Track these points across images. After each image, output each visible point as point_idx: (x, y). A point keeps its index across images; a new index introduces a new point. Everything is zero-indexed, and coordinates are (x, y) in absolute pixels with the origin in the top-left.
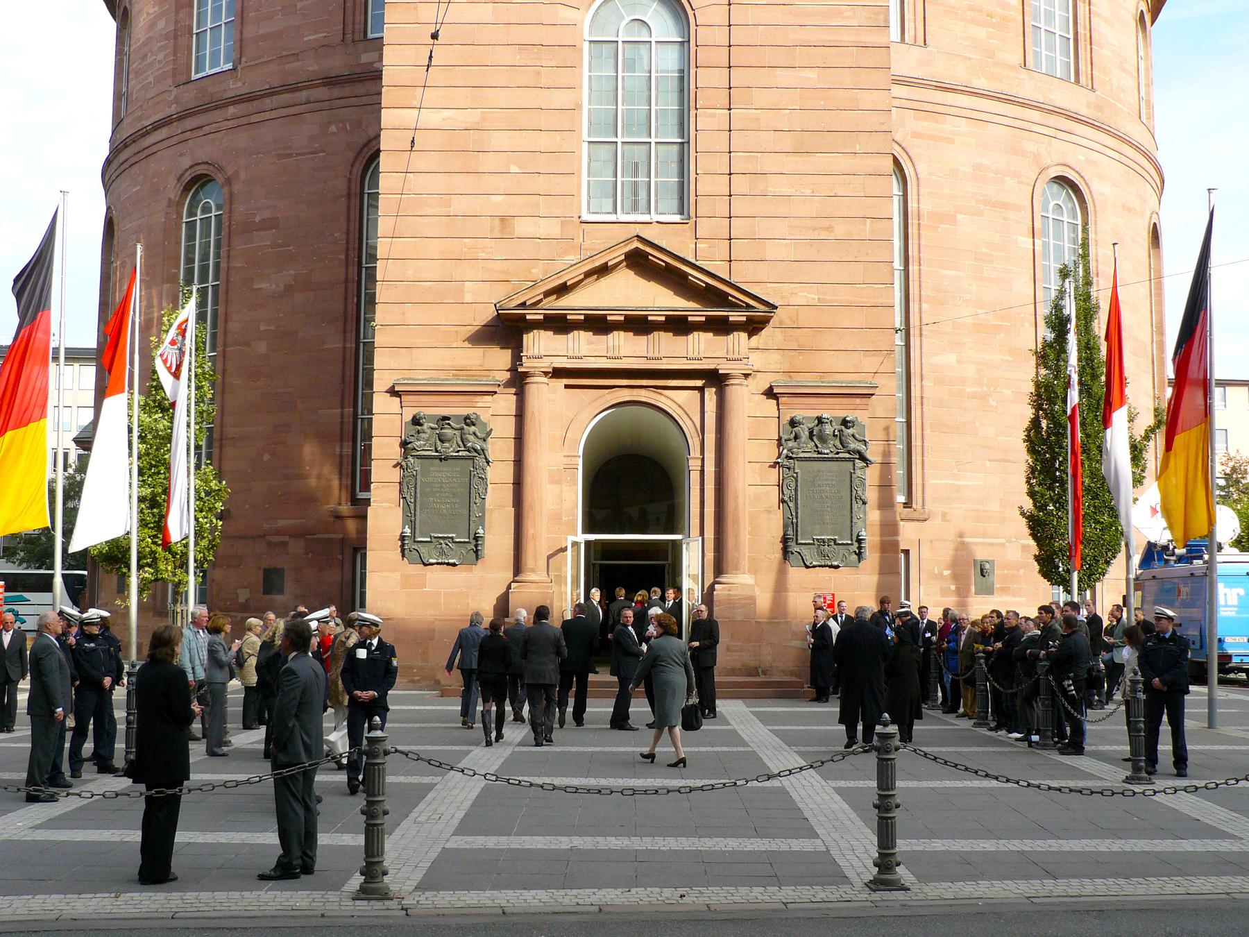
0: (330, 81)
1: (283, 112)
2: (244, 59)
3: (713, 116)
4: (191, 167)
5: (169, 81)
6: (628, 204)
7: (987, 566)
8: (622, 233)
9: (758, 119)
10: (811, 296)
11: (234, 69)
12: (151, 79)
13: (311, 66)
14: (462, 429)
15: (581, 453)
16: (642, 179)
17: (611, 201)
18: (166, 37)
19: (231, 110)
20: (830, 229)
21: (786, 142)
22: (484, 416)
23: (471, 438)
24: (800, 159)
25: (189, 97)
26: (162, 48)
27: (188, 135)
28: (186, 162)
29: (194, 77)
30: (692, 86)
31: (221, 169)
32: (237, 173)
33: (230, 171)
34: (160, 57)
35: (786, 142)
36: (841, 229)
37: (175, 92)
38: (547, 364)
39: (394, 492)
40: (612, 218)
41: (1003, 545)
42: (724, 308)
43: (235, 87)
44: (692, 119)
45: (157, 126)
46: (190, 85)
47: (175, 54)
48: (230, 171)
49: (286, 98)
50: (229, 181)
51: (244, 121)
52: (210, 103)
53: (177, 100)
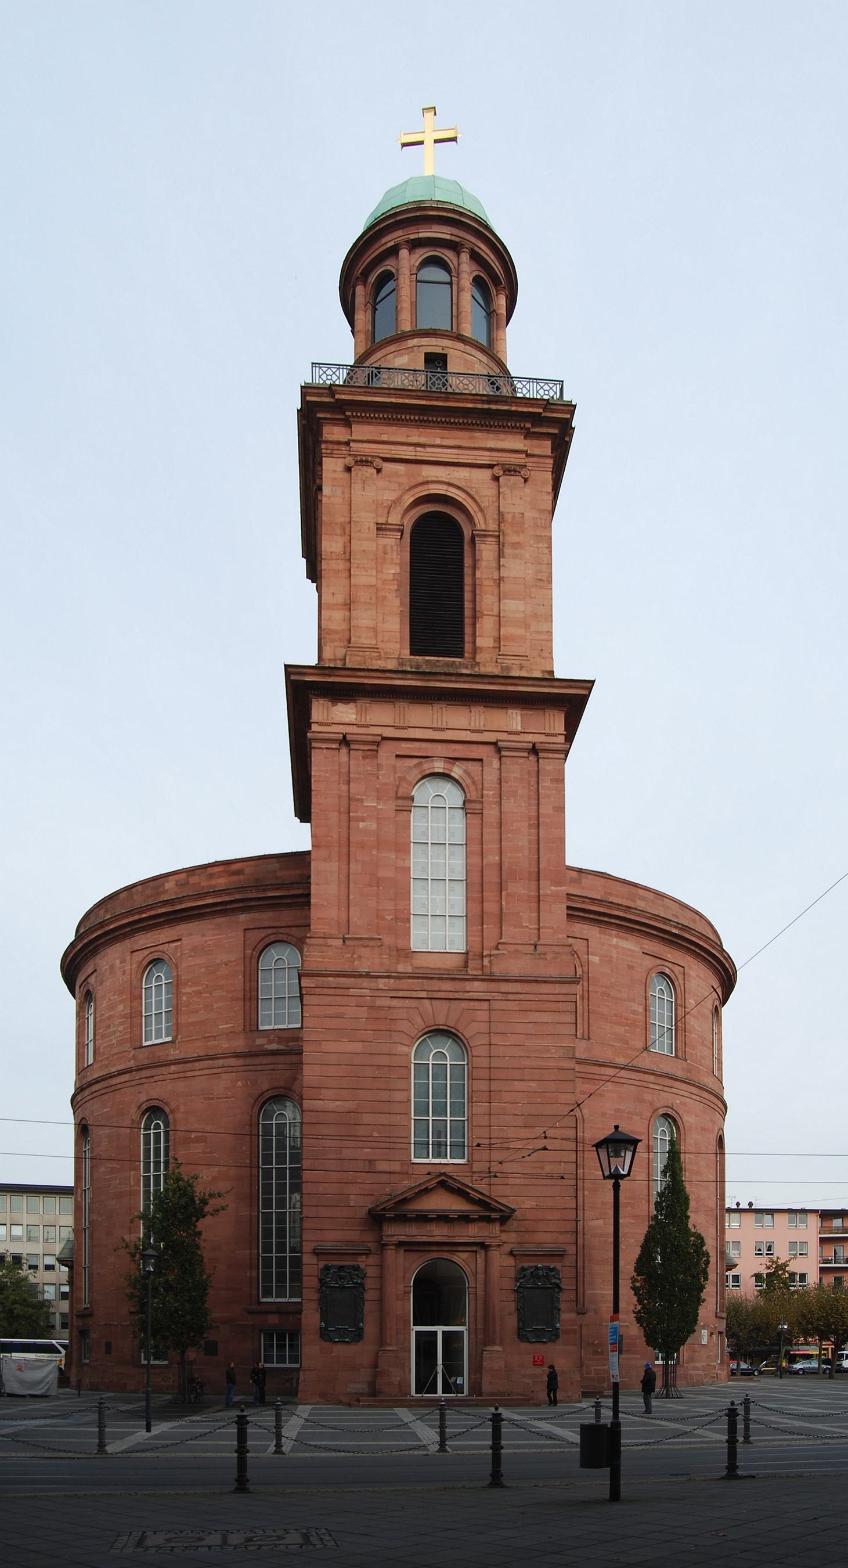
6: (435, 1153)
11: (172, 1042)
12: (114, 1041)
13: (225, 1045)
18: (125, 1016)
25: (143, 1057)
26: (121, 1024)
27: (144, 1081)
28: (143, 1098)
29: (145, 1044)
32: (178, 1107)
33: (173, 1105)
34: (121, 1028)
37: (133, 1052)
43: (174, 1053)
46: (143, 1050)
47: (131, 1027)
48: (173, 1105)
51: (181, 1075)
52: (156, 1063)
53: (134, 1058)
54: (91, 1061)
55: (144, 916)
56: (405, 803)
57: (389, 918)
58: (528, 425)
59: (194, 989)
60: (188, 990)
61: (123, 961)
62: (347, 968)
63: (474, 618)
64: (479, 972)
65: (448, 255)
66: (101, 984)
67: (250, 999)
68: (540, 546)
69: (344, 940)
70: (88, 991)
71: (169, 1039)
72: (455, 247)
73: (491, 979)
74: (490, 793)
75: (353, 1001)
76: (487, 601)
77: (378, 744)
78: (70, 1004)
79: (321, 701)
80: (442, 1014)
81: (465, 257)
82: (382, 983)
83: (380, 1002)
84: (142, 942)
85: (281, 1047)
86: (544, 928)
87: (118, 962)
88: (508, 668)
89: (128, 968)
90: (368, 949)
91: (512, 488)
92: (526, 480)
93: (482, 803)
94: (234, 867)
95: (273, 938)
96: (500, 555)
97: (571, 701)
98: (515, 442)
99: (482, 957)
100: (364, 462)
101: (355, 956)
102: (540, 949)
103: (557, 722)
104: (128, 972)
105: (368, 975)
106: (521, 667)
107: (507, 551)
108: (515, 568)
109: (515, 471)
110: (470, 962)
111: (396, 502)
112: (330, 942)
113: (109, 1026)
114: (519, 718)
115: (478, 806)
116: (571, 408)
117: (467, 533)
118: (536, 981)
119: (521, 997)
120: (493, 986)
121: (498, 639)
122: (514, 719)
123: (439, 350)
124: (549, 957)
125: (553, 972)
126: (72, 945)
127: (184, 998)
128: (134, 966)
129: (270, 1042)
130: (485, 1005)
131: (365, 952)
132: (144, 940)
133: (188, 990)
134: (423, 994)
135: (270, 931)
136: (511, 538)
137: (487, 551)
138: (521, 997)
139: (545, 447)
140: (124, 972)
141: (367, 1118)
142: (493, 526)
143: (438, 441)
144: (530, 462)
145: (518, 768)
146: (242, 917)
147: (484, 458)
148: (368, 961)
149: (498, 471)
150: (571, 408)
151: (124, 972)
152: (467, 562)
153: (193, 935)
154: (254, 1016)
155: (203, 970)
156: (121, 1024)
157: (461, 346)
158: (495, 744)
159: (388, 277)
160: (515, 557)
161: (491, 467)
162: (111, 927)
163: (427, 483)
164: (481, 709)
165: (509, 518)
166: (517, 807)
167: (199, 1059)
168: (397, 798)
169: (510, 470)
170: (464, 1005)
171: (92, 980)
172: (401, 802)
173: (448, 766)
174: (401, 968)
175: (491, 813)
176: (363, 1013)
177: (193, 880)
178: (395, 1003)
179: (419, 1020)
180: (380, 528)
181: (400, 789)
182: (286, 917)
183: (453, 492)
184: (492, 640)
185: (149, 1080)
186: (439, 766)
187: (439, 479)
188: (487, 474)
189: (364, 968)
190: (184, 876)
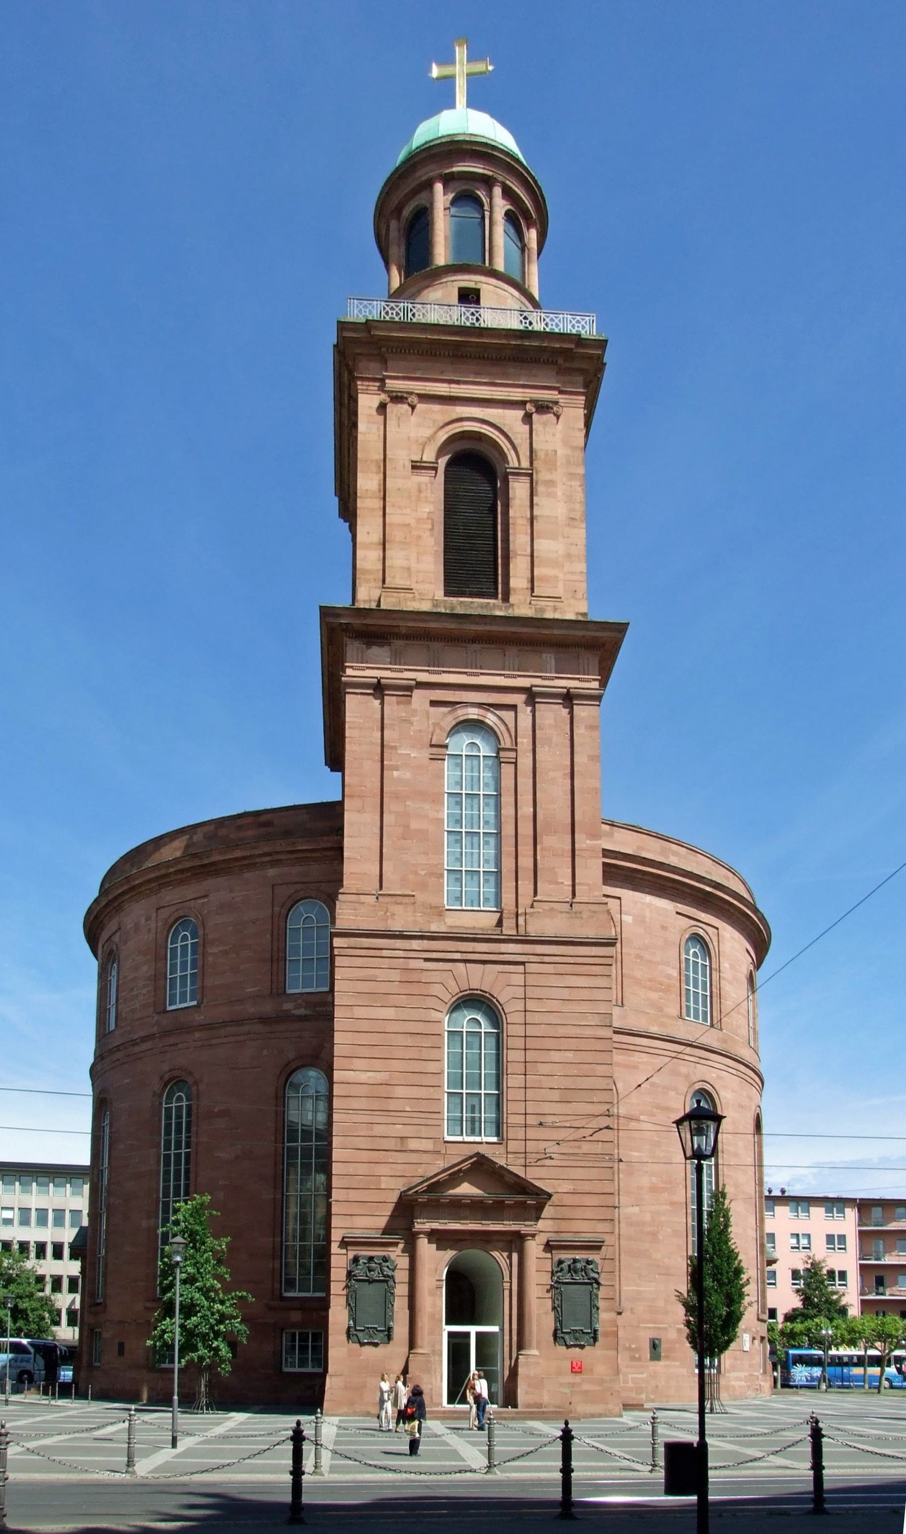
0: (263, 1020)
1: (232, 1039)
2: (205, 1000)
3: (517, 1078)
4: (171, 1070)
5: (151, 1009)
6: (469, 1131)
7: (657, 1342)
9: (540, 1081)
12: (138, 1005)
13: (251, 1009)
14: (380, 1264)
15: (444, 1278)
16: (477, 1115)
17: (459, 1128)
19: (197, 1035)
23: (386, 1269)
26: (144, 986)
29: (169, 1008)
30: (505, 1060)
31: (191, 1074)
34: (144, 991)
37: (156, 1018)
39: (343, 1300)
40: (459, 1139)
41: (666, 1328)
42: (527, 1199)
43: (199, 1018)
44: (505, 1080)
45: (144, 1039)
49: (234, 1029)
50: (196, 1083)
52: (180, 1027)
54: (112, 1027)
55: (172, 870)
57: (423, 873)
59: (221, 948)
60: (215, 950)
61: (148, 919)
64: (514, 933)
66: (125, 943)
67: (278, 960)
68: (573, 484)
70: (111, 952)
71: (195, 1003)
75: (385, 963)
76: (519, 540)
77: (410, 689)
78: (92, 965)
80: (479, 978)
82: (415, 944)
84: (168, 898)
85: (308, 1012)
86: (581, 884)
87: (143, 920)
88: (542, 610)
89: (153, 925)
90: (401, 907)
91: (545, 424)
93: (516, 750)
94: (263, 818)
95: (302, 894)
101: (388, 914)
104: (153, 931)
106: (555, 609)
109: (548, 407)
110: (504, 920)
113: (132, 989)
114: (553, 661)
115: (513, 754)
117: (499, 474)
123: (472, 285)
126: (96, 900)
127: (210, 959)
128: (160, 924)
129: (297, 1007)
130: (521, 968)
131: (398, 910)
132: (170, 896)
133: (215, 950)
134: (457, 956)
135: (298, 887)
136: (542, 475)
137: (518, 489)
140: (149, 931)
141: (400, 1091)
142: (525, 463)
144: (562, 399)
145: (552, 715)
146: (271, 872)
147: (517, 394)
148: (401, 921)
151: (149, 931)
153: (219, 890)
154: (281, 978)
155: (231, 928)
156: (144, 986)
157: (493, 281)
160: (548, 495)
162: (137, 882)
165: (541, 454)
167: (225, 1024)
168: (432, 746)
171: (116, 938)
172: (435, 750)
173: (481, 712)
174: (434, 927)
177: (222, 832)
179: (453, 983)
181: (435, 737)
182: (315, 870)
184: (526, 581)
185: (172, 1048)
186: (473, 713)
190: (212, 828)
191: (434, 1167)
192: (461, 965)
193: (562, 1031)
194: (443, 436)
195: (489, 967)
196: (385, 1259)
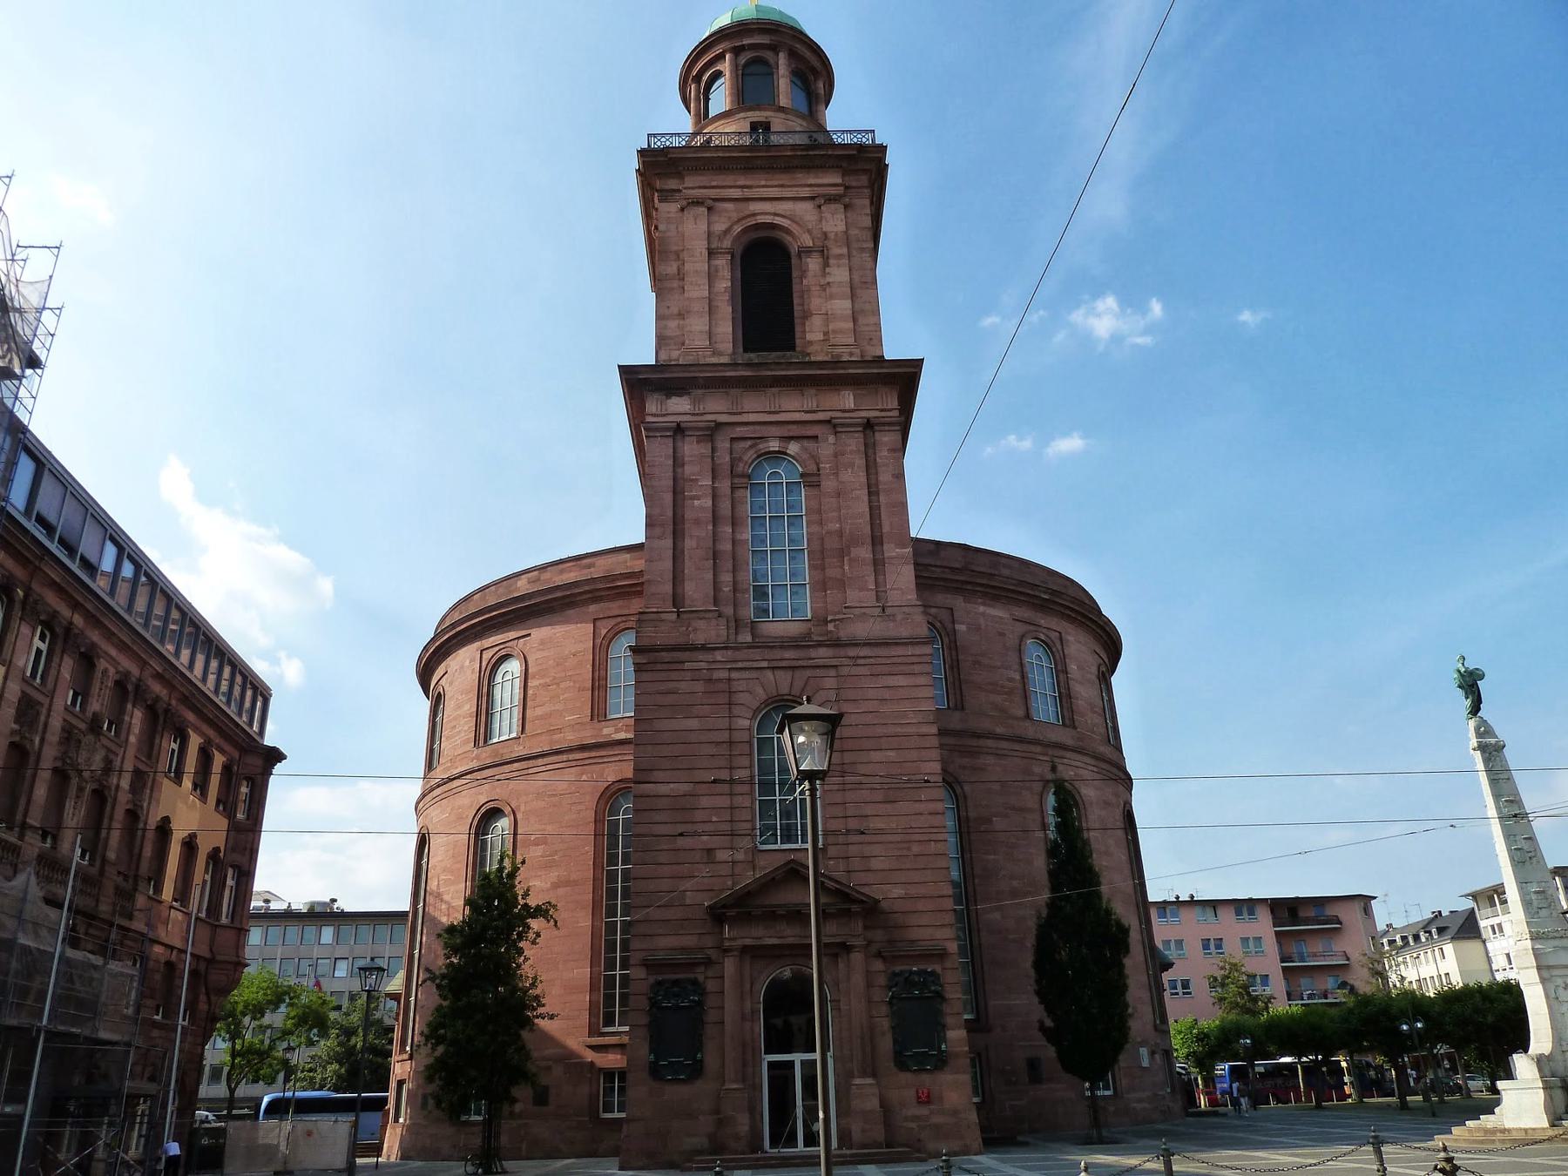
8: (780, 860)
10: (897, 892)
20: (909, 849)
21: (879, 796)
22: (701, 978)
24: (888, 806)
35: (879, 796)
36: (916, 849)
38: (739, 942)
56: (742, 479)
58: (844, 165)
62: (681, 640)
63: (807, 315)
65: (768, 55)
69: (679, 613)
72: (774, 48)
73: (837, 644)
74: (825, 466)
76: (816, 302)
79: (656, 396)
81: (782, 59)
83: (716, 675)
92: (846, 207)
96: (826, 264)
97: (905, 378)
98: (834, 178)
99: (826, 622)
100: (698, 202)
102: (888, 611)
103: (890, 401)
105: (704, 648)
106: (851, 354)
107: (832, 261)
108: (839, 274)
111: (726, 232)
112: (663, 616)
116: (882, 149)
117: (794, 249)
118: (887, 644)
119: (872, 661)
120: (842, 652)
121: (826, 334)
122: (847, 399)
124: (899, 617)
125: (904, 632)
130: (832, 672)
134: (765, 664)
136: (835, 251)
137: (813, 264)
138: (872, 661)
139: (864, 179)
141: (705, 802)
143: (764, 185)
147: (806, 192)
149: (817, 202)
150: (882, 149)
152: (795, 274)
158: (829, 422)
159: (717, 75)
161: (813, 198)
163: (754, 215)
164: (813, 391)
165: (832, 236)
166: (854, 477)
169: (830, 199)
170: (808, 673)
174: (741, 638)
175: (828, 484)
176: (699, 687)
178: (734, 675)
179: (761, 691)
180: (711, 253)
183: (778, 221)
186: (774, 445)
187: (764, 212)
188: (808, 206)
189: (699, 638)
191: (748, 878)
192: (769, 674)
193: (880, 731)
194: (738, 229)
195: (798, 673)
196: (695, 982)
